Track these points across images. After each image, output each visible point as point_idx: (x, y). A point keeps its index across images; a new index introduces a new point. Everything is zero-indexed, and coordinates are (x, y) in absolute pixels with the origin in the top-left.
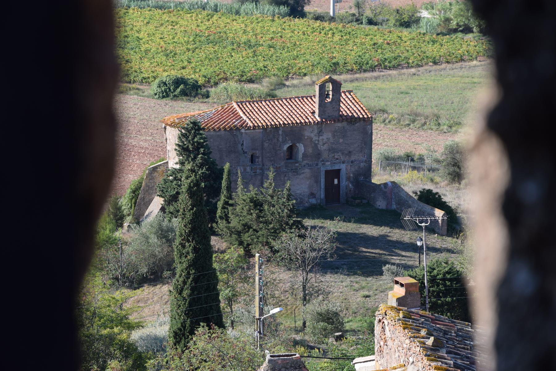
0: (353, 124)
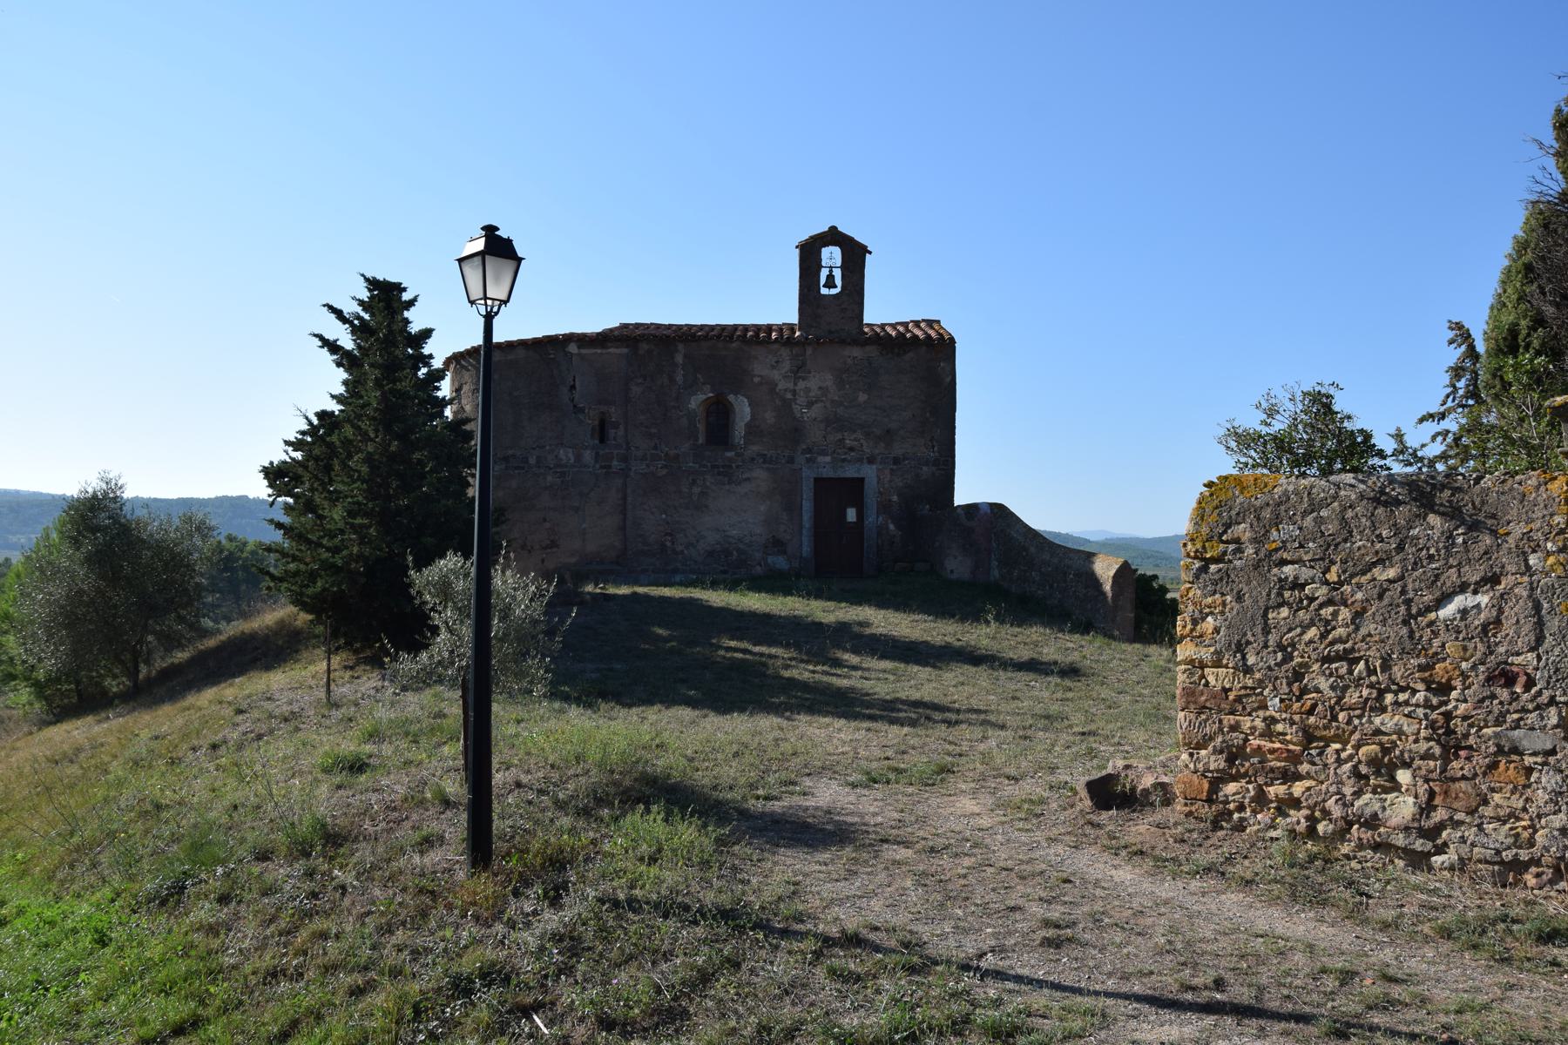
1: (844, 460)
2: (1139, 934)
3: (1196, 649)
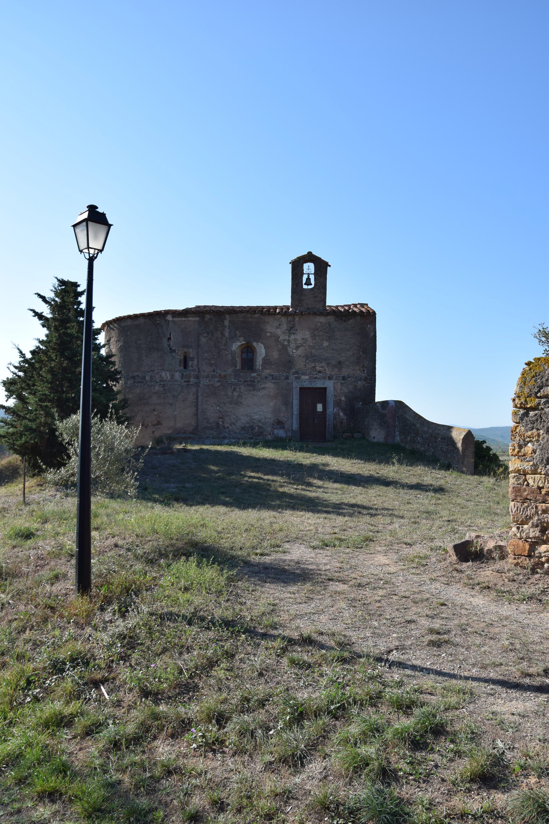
0: (345, 321)
1: (315, 378)
2: (491, 638)
3: (522, 463)
